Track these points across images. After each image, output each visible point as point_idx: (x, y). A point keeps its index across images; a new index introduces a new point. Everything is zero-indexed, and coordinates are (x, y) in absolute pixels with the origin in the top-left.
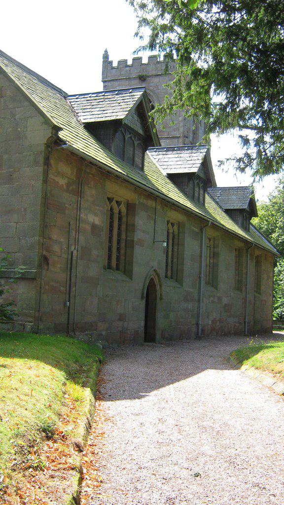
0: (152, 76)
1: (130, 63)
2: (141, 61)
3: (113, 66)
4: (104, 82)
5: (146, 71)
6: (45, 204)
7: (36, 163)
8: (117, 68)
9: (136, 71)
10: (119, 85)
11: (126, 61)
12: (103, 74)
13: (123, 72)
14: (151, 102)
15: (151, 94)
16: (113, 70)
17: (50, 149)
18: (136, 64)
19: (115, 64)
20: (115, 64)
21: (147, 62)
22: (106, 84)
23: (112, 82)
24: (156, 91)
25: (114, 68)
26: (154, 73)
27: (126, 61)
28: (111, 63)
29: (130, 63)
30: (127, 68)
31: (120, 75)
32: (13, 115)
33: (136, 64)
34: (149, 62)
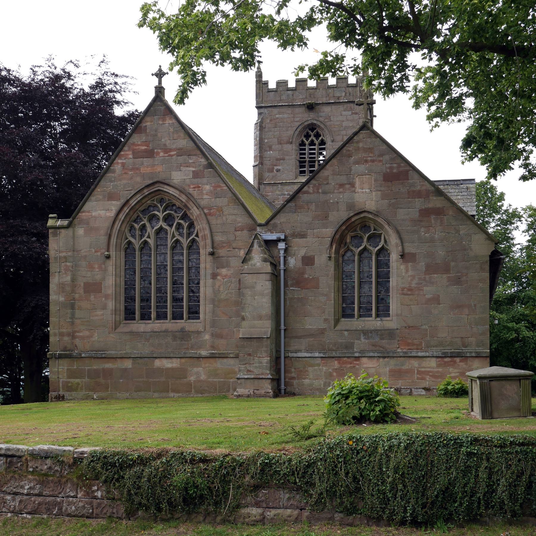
0: (323, 104)
1: (292, 84)
2: (268, 86)
3: (289, 86)
4: (258, 107)
5: (315, 98)
6: (254, 525)
7: (200, 361)
8: (276, 91)
9: (301, 97)
10: (279, 113)
11: (285, 82)
12: (257, 98)
13: (284, 97)
14: (320, 136)
15: (322, 126)
16: (270, 93)
17: (103, 266)
18: (301, 87)
19: (272, 85)
20: (272, 85)
21: (294, 86)
22: (262, 110)
23: (270, 109)
24: (328, 124)
25: (292, 89)
26: (324, 100)
27: (285, 82)
28: (266, 83)
29: (292, 84)
30: (289, 92)
31: (281, 100)
32: (458, 231)
33: (301, 87)
34: (296, 87)
